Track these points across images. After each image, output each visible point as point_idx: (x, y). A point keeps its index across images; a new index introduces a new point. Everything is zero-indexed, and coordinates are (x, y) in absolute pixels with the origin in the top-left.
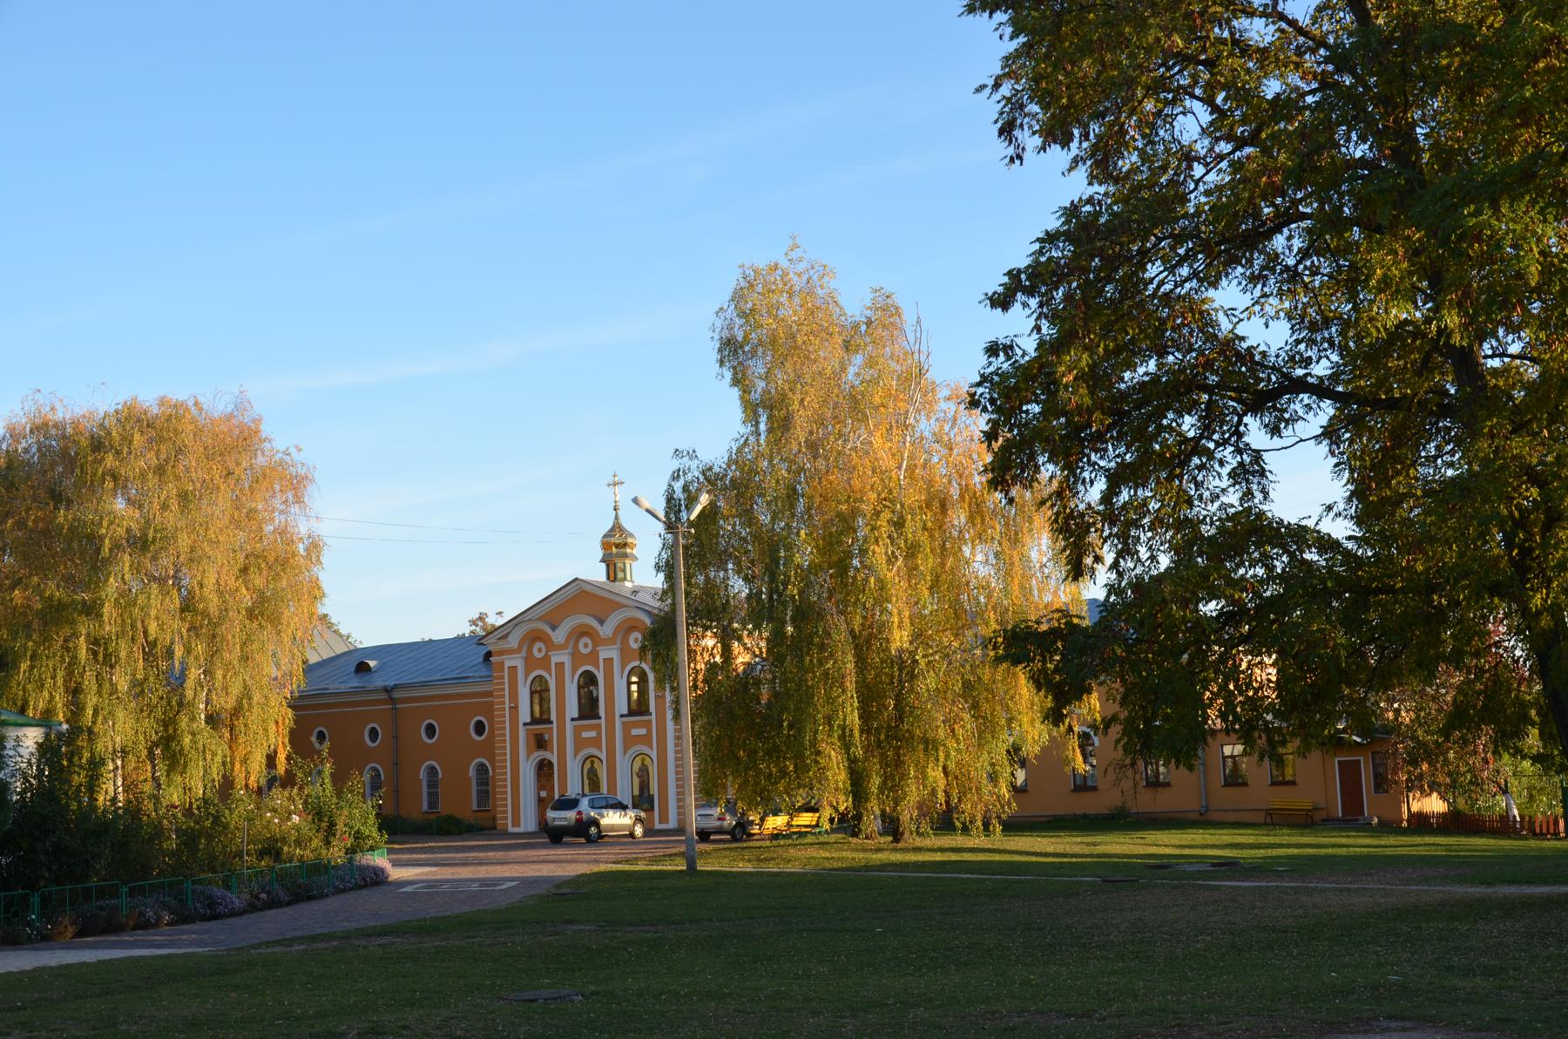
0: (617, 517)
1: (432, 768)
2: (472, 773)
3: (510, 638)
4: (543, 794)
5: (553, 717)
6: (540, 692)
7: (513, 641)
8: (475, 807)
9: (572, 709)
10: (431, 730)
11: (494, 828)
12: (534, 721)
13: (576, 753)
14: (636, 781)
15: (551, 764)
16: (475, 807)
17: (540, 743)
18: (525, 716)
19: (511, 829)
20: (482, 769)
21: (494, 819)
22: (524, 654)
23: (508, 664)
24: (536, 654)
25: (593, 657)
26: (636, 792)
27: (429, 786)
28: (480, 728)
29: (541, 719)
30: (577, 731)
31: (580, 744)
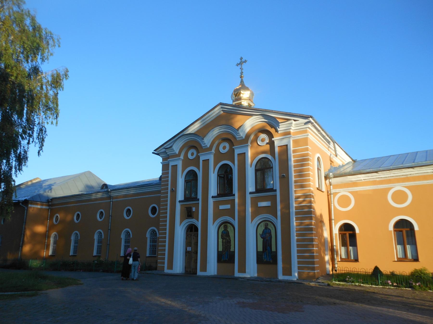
0: (242, 82)
1: (128, 232)
2: (148, 235)
3: (174, 147)
4: (189, 249)
5: (200, 196)
6: (191, 178)
7: (176, 148)
8: (148, 255)
9: (213, 190)
10: (129, 211)
11: (156, 269)
12: (187, 199)
13: (214, 221)
14: (260, 240)
15: (196, 229)
16: (148, 255)
17: (189, 213)
18: (180, 196)
19: (166, 271)
20: (153, 233)
21: (157, 262)
22: (182, 157)
23: (171, 164)
24: (190, 156)
25: (230, 155)
26: (260, 249)
27: (125, 242)
28: (154, 210)
29: (191, 196)
30: (216, 205)
31: (218, 214)
